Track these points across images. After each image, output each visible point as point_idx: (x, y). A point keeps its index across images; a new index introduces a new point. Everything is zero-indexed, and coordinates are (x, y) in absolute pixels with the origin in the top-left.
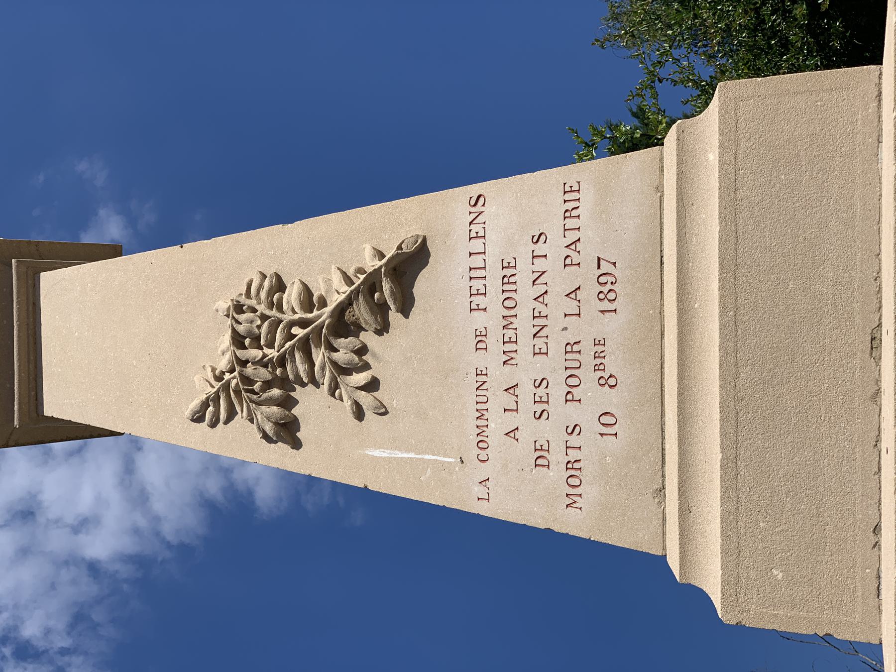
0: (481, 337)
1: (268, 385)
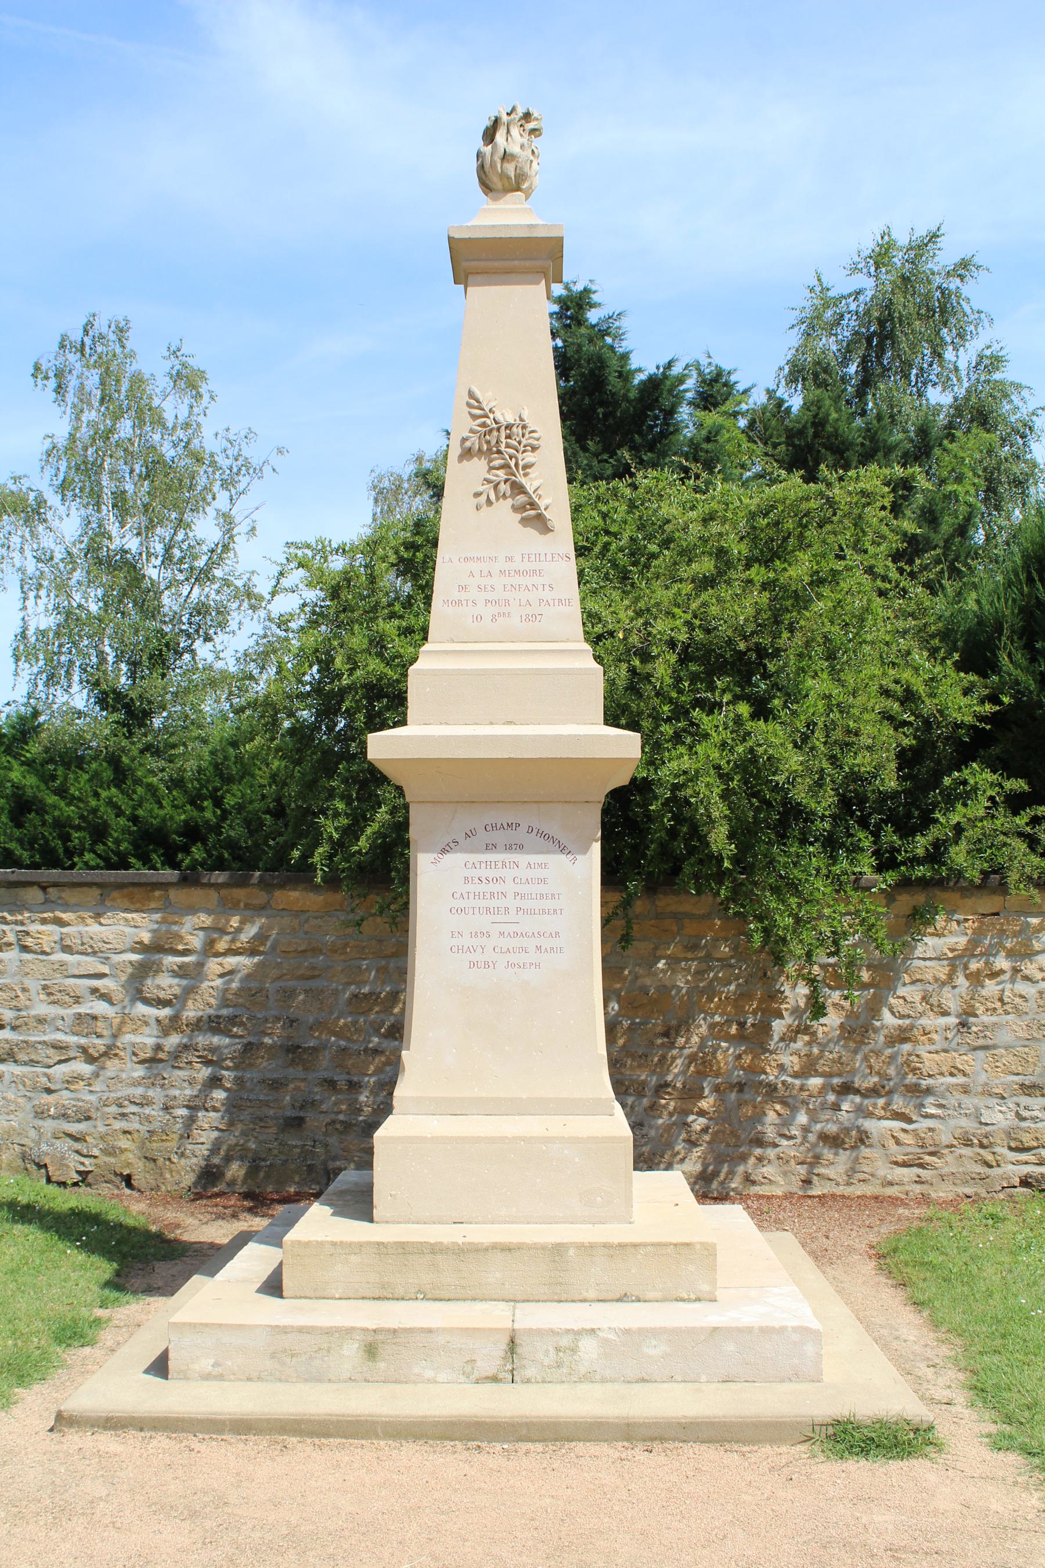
0: (510, 559)
1: (488, 442)
